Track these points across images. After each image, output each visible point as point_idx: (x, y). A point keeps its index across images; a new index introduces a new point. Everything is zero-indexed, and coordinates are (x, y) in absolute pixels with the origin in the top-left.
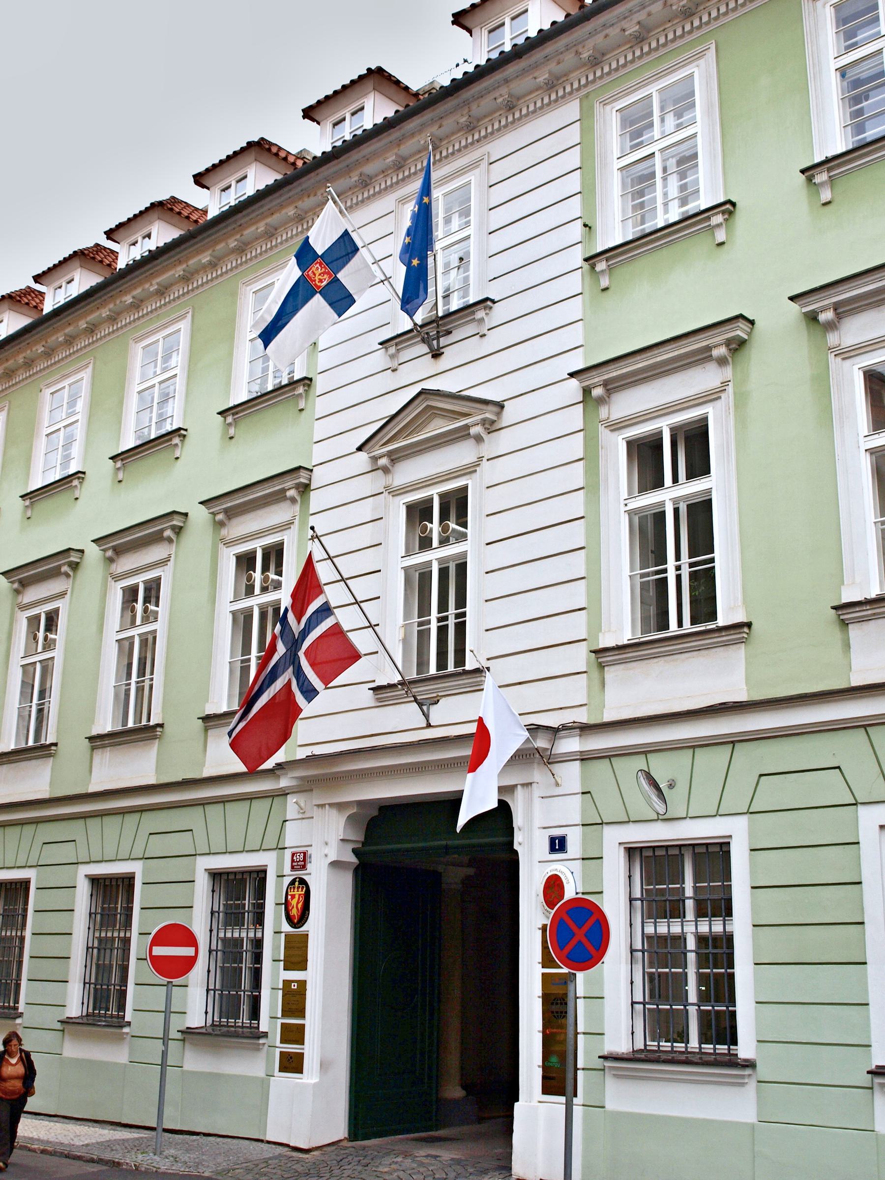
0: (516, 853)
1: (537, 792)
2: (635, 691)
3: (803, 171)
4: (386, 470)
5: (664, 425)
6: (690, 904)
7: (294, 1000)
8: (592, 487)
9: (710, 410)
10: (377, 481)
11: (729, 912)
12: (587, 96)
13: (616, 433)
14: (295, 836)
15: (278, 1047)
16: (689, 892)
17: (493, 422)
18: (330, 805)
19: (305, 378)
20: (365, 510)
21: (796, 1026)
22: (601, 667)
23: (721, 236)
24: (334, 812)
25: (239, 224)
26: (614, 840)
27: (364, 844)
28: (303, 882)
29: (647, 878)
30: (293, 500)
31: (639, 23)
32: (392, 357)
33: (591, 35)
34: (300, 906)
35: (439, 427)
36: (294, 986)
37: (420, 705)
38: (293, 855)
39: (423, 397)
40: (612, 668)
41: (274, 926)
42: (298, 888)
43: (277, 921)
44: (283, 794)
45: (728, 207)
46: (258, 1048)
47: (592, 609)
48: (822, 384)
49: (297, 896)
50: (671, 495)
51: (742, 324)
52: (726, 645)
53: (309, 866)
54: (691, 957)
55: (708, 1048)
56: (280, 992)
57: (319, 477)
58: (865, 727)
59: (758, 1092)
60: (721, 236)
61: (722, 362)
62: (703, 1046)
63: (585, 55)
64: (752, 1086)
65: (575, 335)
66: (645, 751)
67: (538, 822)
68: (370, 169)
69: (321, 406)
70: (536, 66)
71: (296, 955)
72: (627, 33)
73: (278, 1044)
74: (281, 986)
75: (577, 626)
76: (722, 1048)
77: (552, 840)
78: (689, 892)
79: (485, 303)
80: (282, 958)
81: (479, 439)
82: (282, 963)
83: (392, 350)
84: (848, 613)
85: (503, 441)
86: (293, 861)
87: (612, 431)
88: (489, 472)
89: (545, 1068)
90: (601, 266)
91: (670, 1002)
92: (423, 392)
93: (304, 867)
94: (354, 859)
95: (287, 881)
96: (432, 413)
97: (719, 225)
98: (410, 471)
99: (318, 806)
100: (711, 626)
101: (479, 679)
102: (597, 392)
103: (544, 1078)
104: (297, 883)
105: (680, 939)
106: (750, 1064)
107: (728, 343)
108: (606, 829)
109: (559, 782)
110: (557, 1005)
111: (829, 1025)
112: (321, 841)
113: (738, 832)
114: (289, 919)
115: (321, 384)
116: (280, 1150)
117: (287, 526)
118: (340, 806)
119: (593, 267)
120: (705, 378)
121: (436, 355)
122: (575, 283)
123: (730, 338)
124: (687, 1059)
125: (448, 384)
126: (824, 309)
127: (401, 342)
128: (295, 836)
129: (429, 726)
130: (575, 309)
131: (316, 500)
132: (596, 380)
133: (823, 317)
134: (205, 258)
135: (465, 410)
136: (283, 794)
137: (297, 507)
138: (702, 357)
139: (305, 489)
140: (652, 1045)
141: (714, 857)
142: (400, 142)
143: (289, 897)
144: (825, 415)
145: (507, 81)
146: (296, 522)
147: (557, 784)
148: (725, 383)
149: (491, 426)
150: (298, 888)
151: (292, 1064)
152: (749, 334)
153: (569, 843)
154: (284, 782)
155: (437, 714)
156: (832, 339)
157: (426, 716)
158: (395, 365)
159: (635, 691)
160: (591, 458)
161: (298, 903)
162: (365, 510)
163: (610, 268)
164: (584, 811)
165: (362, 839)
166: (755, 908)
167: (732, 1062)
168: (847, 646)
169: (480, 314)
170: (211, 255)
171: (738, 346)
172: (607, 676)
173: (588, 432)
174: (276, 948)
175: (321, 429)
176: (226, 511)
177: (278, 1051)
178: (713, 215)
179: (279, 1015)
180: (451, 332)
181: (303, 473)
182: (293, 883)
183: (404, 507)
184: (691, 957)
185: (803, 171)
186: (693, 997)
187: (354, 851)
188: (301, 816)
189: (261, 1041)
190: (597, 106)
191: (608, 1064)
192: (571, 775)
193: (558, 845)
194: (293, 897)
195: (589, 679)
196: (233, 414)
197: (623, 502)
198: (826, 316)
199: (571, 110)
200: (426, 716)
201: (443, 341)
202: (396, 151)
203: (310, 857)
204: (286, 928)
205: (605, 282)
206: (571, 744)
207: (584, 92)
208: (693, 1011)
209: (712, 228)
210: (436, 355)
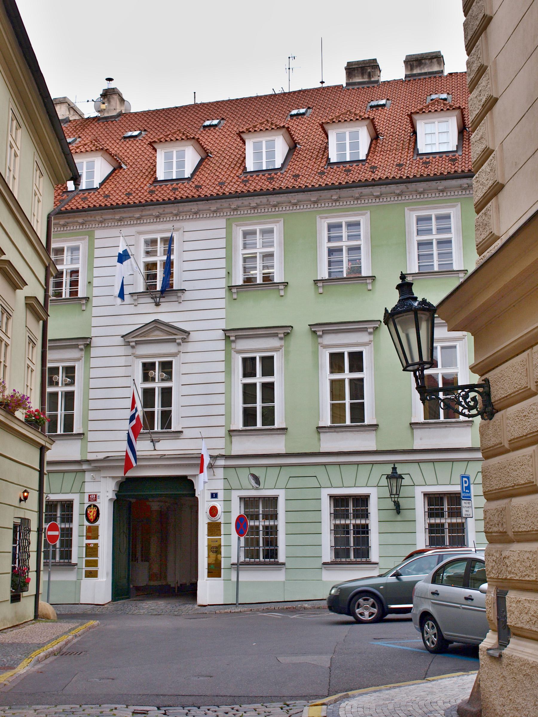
0: (197, 498)
2: (242, 446)
3: (314, 281)
4: (133, 347)
5: (258, 355)
6: (261, 516)
7: (92, 551)
8: (228, 371)
9: (276, 355)
10: (129, 351)
11: (276, 518)
12: (229, 219)
14: (90, 488)
15: (85, 569)
16: (261, 512)
17: (185, 338)
18: (109, 477)
20: (122, 361)
21: (299, 551)
22: (231, 436)
23: (282, 293)
24: (111, 480)
26: (235, 495)
28: (95, 506)
29: (245, 508)
30: (81, 350)
32: (135, 300)
34: (94, 515)
35: (158, 335)
36: (92, 546)
37: (152, 441)
38: (89, 496)
40: (235, 437)
41: (78, 524)
43: (81, 520)
44: (84, 471)
45: (286, 284)
46: (72, 570)
47: (228, 415)
48: (316, 355)
50: (259, 380)
51: (290, 328)
52: (279, 434)
53: (98, 500)
54: (261, 533)
55: (267, 560)
56: (84, 549)
57: (95, 342)
58: (325, 465)
59: (285, 571)
60: (282, 293)
61: (281, 339)
63: (233, 207)
64: (284, 570)
66: (249, 467)
68: (124, 215)
69: (95, 311)
71: (92, 533)
73: (84, 567)
74: (85, 545)
75: (221, 421)
76: (272, 560)
77: (212, 494)
78: (261, 512)
79: (183, 291)
80: (85, 534)
81: (179, 344)
82: (85, 537)
83: (136, 297)
84: (320, 429)
85: (189, 347)
86: (89, 498)
88: (183, 358)
89: (208, 569)
90: (234, 290)
92: (156, 321)
93: (96, 500)
94: (115, 498)
95: (86, 506)
98: (143, 350)
100: (272, 427)
102: (232, 338)
103: (208, 572)
105: (257, 527)
106: (283, 564)
107: (284, 333)
108: (233, 491)
110: (215, 549)
111: (309, 552)
112: (105, 491)
113: (281, 494)
114: (88, 520)
115: (95, 301)
116: (93, 606)
117: (78, 360)
118: (113, 478)
119: (230, 289)
120: (274, 343)
121: (157, 304)
122: (222, 293)
123: (285, 332)
125: (165, 318)
126: (319, 331)
128: (90, 488)
129: (155, 450)
130: (222, 303)
131: (94, 352)
133: (318, 333)
135: (174, 332)
136: (84, 471)
137: (83, 353)
138: (275, 335)
139: (88, 346)
140: (247, 560)
141: (273, 501)
144: (316, 365)
146: (83, 359)
147: (214, 475)
148: (282, 346)
149: (184, 340)
151: (91, 574)
152: (291, 331)
153: (216, 496)
154: (85, 467)
155: (158, 446)
156: (320, 340)
157: (154, 446)
158: (136, 303)
159: (242, 446)
160: (228, 361)
162: (122, 361)
163: (237, 292)
164: (224, 486)
165: (118, 490)
166: (286, 517)
167: (277, 564)
168: (319, 439)
169: (179, 294)
171: (287, 334)
172: (233, 440)
173: (228, 352)
174: (81, 531)
179: (84, 556)
181: (89, 340)
182: (90, 506)
184: (261, 533)
185: (314, 281)
186: (261, 545)
187: (116, 495)
190: (234, 226)
191: (233, 566)
192: (220, 473)
193: (214, 496)
194: (91, 512)
195: (226, 440)
197: (240, 380)
198: (320, 333)
199: (221, 223)
200: (154, 446)
203: (99, 496)
204: (86, 523)
205: (235, 296)
206: (221, 462)
208: (261, 549)
209: (279, 290)
210: (157, 304)
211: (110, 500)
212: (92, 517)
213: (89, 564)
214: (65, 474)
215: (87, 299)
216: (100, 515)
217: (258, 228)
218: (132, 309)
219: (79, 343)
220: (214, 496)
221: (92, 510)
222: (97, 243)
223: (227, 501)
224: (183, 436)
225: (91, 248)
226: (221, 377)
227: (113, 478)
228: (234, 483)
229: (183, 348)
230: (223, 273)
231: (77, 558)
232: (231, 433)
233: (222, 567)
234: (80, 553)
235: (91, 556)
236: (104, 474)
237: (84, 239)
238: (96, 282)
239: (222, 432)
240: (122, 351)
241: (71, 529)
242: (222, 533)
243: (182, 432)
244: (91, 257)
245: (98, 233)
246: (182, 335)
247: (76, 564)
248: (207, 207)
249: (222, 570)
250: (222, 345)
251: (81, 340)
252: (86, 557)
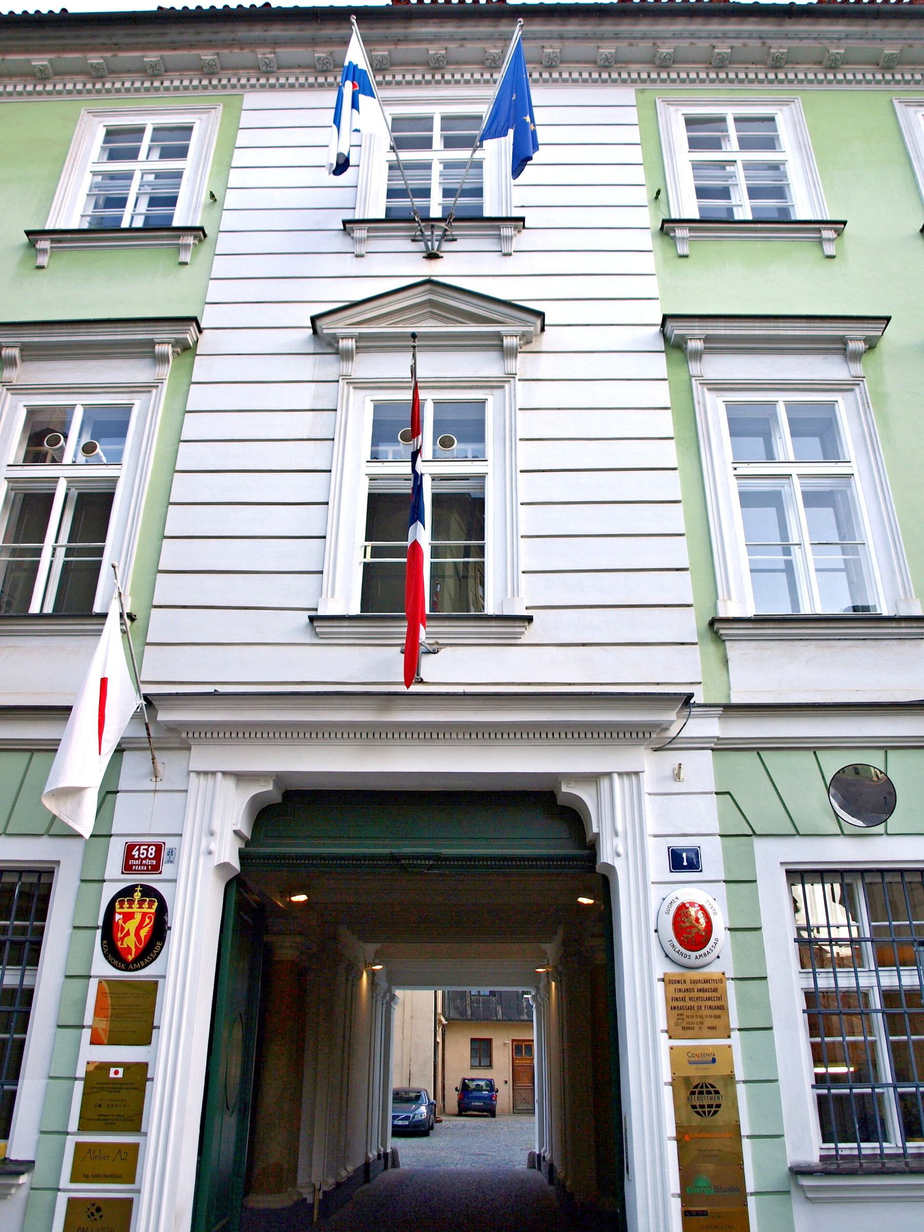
1: (648, 783)
7: (116, 1101)
10: (330, 367)
13: (714, 394)
14: (135, 818)
18: (225, 773)
19: (201, 229)
20: (305, 396)
24: (227, 787)
25: (114, 40)
26: (770, 858)
27: (248, 843)
28: (149, 892)
31: (732, 48)
33: (676, 36)
34: (144, 933)
38: (130, 848)
39: (428, 287)
41: (64, 965)
42: (141, 903)
49: (138, 917)
52: (901, 638)
53: (166, 868)
56: (79, 1087)
60: (829, 249)
62: (908, 1144)
65: (650, 287)
66: (815, 747)
67: (651, 827)
69: (220, 267)
70: (602, 38)
71: (131, 1014)
72: (716, 51)
73: (65, 1181)
74: (81, 1072)
75: (680, 588)
82: (87, 1034)
85: (544, 366)
86: (128, 855)
87: (709, 389)
88: (524, 394)
89: (684, 1196)
91: (829, 1084)
92: (429, 282)
93: (156, 868)
94: (236, 864)
95: (109, 891)
96: (435, 309)
97: (829, 240)
99: (198, 773)
101: (518, 630)
103: (686, 1214)
104: (137, 895)
108: (759, 845)
109: (682, 776)
114: (113, 953)
115: (224, 243)
117: (146, 388)
118: (240, 777)
120: (831, 368)
122: (646, 240)
124: (882, 1167)
127: (376, 229)
130: (648, 263)
131: (202, 369)
132: (697, 332)
134: (40, 61)
137: (165, 371)
139: (187, 349)
142: (398, 41)
143: (118, 917)
145: (561, 37)
146: (165, 387)
147: (677, 776)
150: (141, 903)
161: (140, 927)
162: (305, 396)
164: (722, 819)
169: (506, 231)
170: (50, 61)
175: (215, 291)
176: (24, 347)
178: (825, 229)
179: (73, 1125)
180: (456, 240)
181: (193, 328)
182: (127, 892)
183: (371, 405)
184: (879, 1020)
188: (151, 786)
189: (23, 1179)
193: (683, 861)
194: (128, 917)
195: (703, 654)
196: (53, 241)
197: (730, 467)
201: (446, 246)
202: (392, 47)
203: (171, 852)
204: (102, 967)
207: (642, 86)
208: (890, 1096)
210: (432, 256)
211: (224, 866)
212: (130, 942)
213: (89, 1163)
214: (36, 754)
215: (198, 232)
216: (174, 938)
217: (730, 112)
218: (349, 265)
219: (157, 337)
220: (683, 861)
222: (246, 119)
223: (741, 882)
224: (530, 634)
225: (231, 128)
226: (668, 454)
227: (240, 777)
228: (763, 810)
229: (522, 365)
230: (643, 196)
231: (35, 1136)
232: (717, 628)
233: (750, 1186)
234: (55, 1103)
235: (109, 1125)
236: (202, 757)
237: (207, 110)
238: (231, 199)
239: (688, 625)
240: (307, 368)
241: (28, 995)
242: (734, 1022)
243: (530, 619)
244: (228, 145)
245: (251, 99)
246: (525, 323)
247: (28, 1166)
248: (585, 49)
249: (751, 1201)
250: (658, 365)
251: (166, 327)
252: (83, 1127)
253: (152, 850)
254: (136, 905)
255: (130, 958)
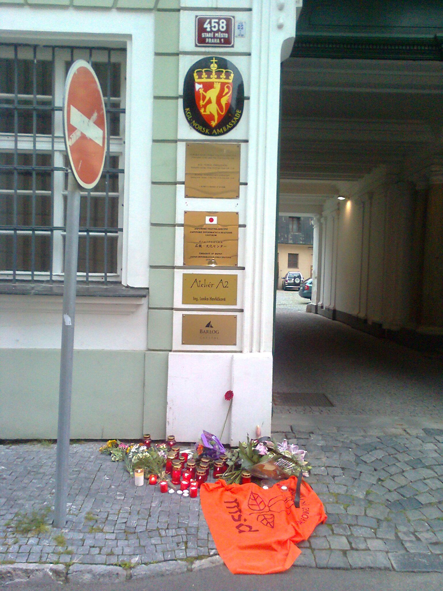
38: (201, 22)
49: (218, 87)
56: (180, 232)
74: (180, 219)
80: (181, 176)
86: (201, 29)
93: (227, 42)
104: (214, 67)
143: (198, 87)
150: (219, 73)
151: (211, 332)
177: (178, 318)
179: (179, 261)
182: (203, 65)
194: (208, 87)
204: (187, 132)
221: (213, 78)
253: (223, 24)
254: (214, 75)
255: (214, 124)
